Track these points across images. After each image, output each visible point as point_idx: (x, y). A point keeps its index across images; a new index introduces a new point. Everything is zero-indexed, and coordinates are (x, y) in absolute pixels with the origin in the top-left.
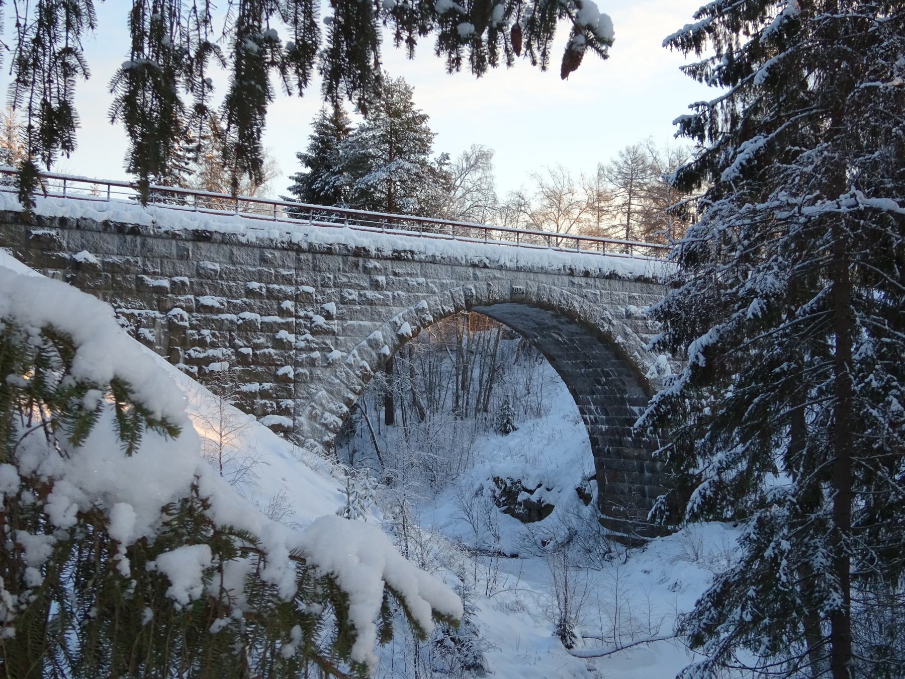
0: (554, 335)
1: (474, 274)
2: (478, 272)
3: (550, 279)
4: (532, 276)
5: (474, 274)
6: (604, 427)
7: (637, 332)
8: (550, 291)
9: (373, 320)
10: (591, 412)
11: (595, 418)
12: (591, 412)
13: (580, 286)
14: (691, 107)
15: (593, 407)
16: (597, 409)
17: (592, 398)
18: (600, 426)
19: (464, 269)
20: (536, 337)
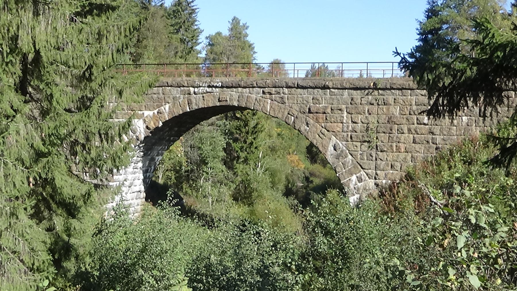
2: (196, 90)
4: (235, 89)
7: (318, 122)
13: (270, 94)
19: (188, 88)
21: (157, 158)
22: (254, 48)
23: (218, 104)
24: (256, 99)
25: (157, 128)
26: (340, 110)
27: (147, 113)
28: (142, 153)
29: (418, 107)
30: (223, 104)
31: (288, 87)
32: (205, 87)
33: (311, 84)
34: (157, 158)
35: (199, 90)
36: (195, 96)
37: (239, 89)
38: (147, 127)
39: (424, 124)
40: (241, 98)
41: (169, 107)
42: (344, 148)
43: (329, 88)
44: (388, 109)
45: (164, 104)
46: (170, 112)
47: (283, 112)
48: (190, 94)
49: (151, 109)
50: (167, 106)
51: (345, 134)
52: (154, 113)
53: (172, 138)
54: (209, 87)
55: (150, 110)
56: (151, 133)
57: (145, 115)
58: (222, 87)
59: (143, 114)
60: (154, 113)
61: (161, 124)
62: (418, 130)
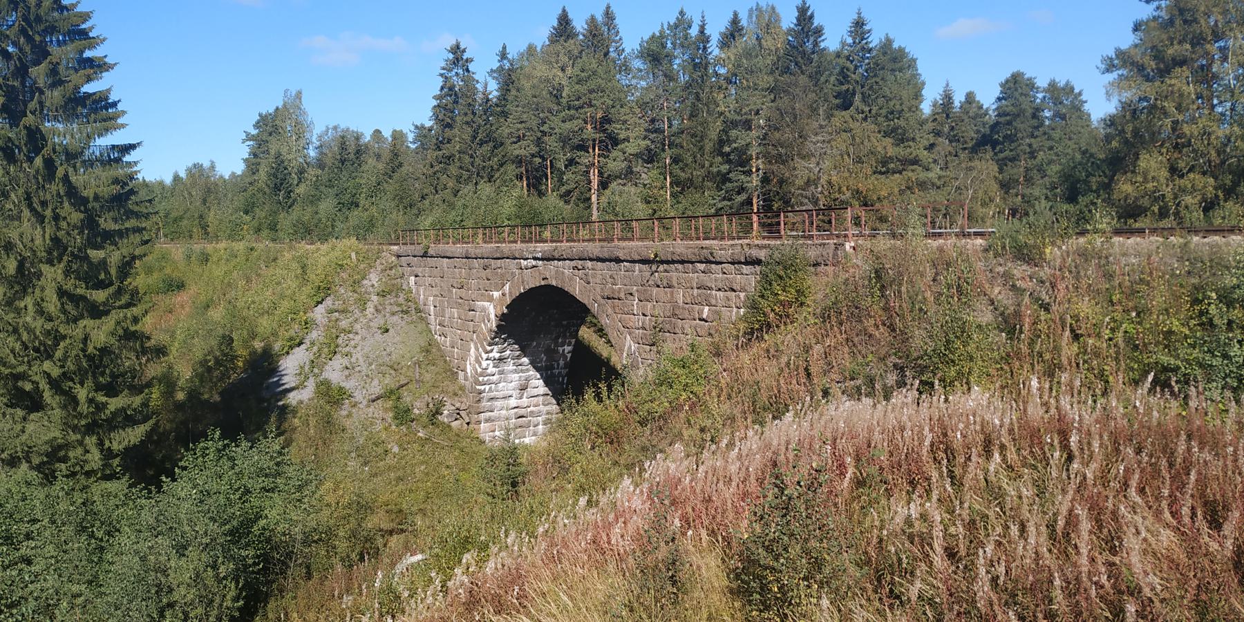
2: (525, 262)
21: (561, 349)
22: (1080, 94)
23: (543, 283)
25: (503, 314)
26: (631, 294)
27: (496, 294)
28: (517, 346)
29: (700, 291)
31: (591, 260)
33: (606, 256)
34: (561, 349)
37: (556, 262)
38: (496, 316)
39: (703, 320)
42: (637, 354)
43: (622, 261)
44: (672, 293)
46: (510, 293)
47: (589, 296)
48: (521, 269)
50: (507, 288)
51: (637, 331)
53: (565, 323)
54: (535, 259)
56: (500, 320)
58: (542, 259)
61: (505, 311)
62: (698, 330)
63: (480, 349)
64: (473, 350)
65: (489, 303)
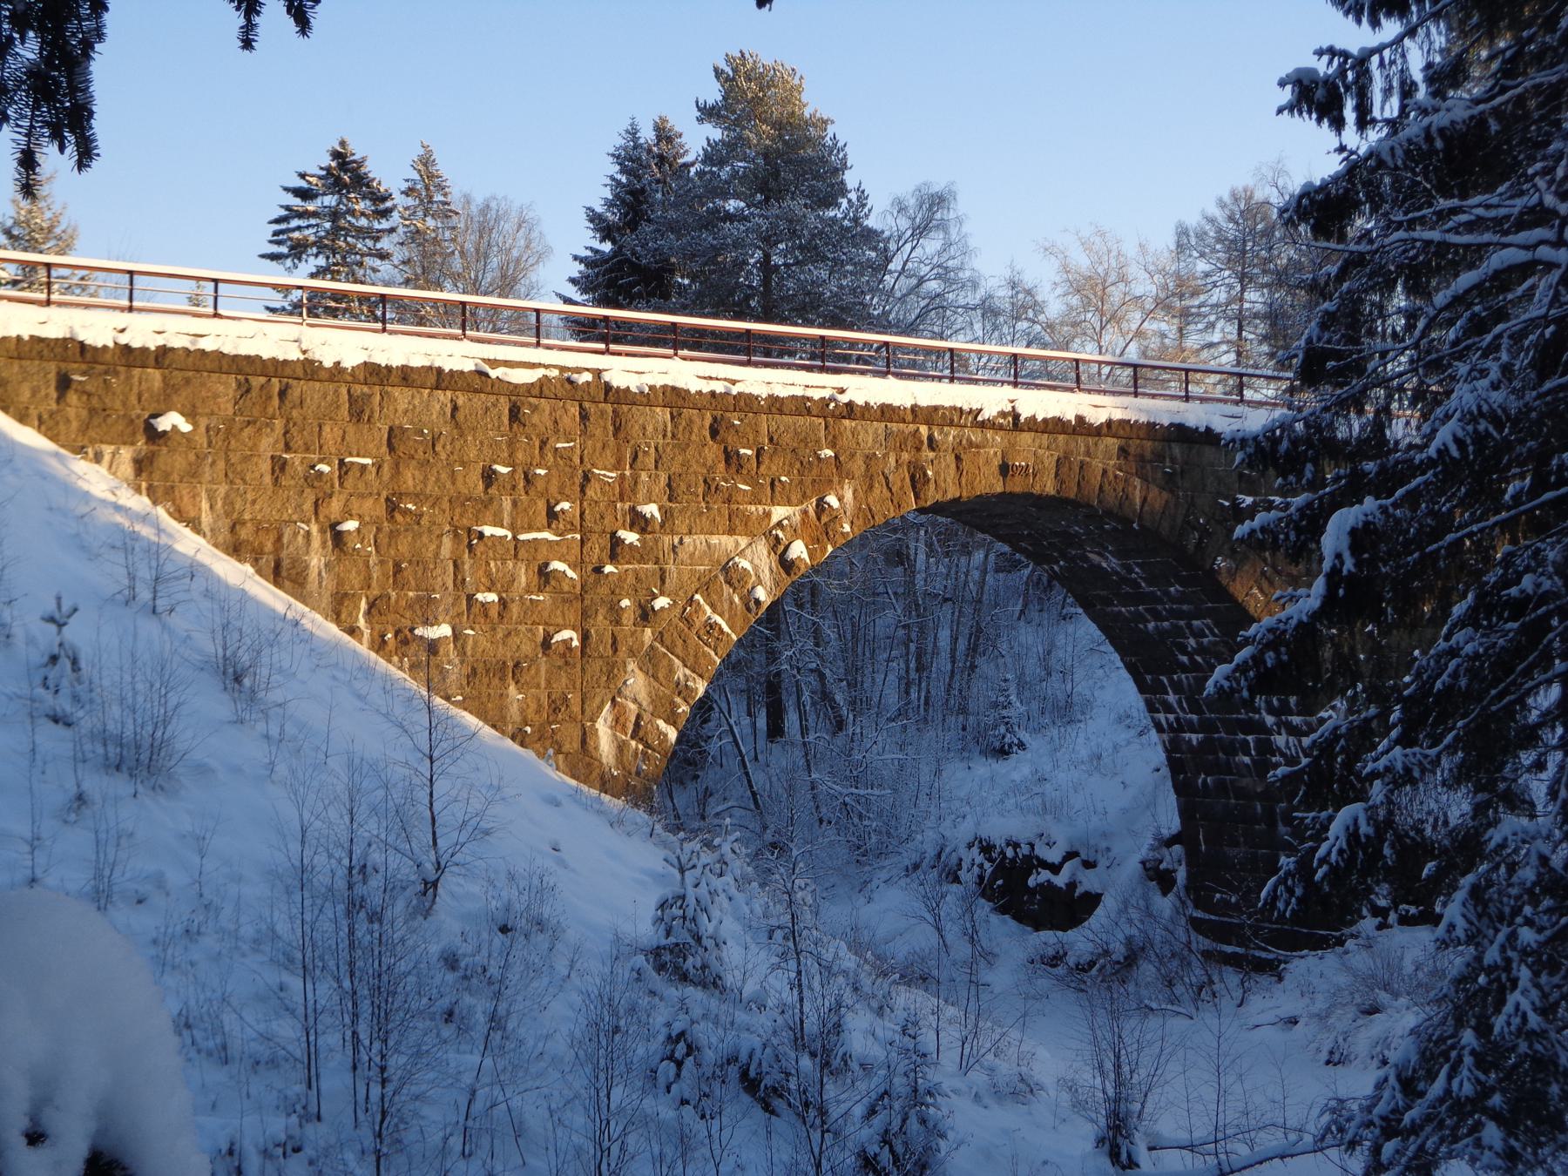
0: (1091, 556)
1: (931, 438)
3: (1081, 443)
5: (931, 438)
6: (1195, 738)
8: (1081, 467)
9: (731, 531)
10: (1168, 709)
11: (1177, 719)
12: (1168, 709)
14: (1320, 53)
15: (1172, 698)
16: (1180, 702)
17: (1171, 680)
18: (1187, 736)
19: (912, 427)
20: (1057, 563)
24: (1105, 472)
27: (779, 513)
30: (1017, 485)
32: (965, 426)
35: (947, 435)
36: (931, 455)
37: (1061, 437)
40: (1065, 469)
41: (855, 491)
45: (836, 479)
46: (863, 511)
49: (794, 499)
50: (848, 495)
52: (805, 512)
55: (789, 503)
57: (775, 519)
59: (768, 515)
60: (805, 512)
63: (681, 672)
64: (636, 682)
65: (743, 541)
